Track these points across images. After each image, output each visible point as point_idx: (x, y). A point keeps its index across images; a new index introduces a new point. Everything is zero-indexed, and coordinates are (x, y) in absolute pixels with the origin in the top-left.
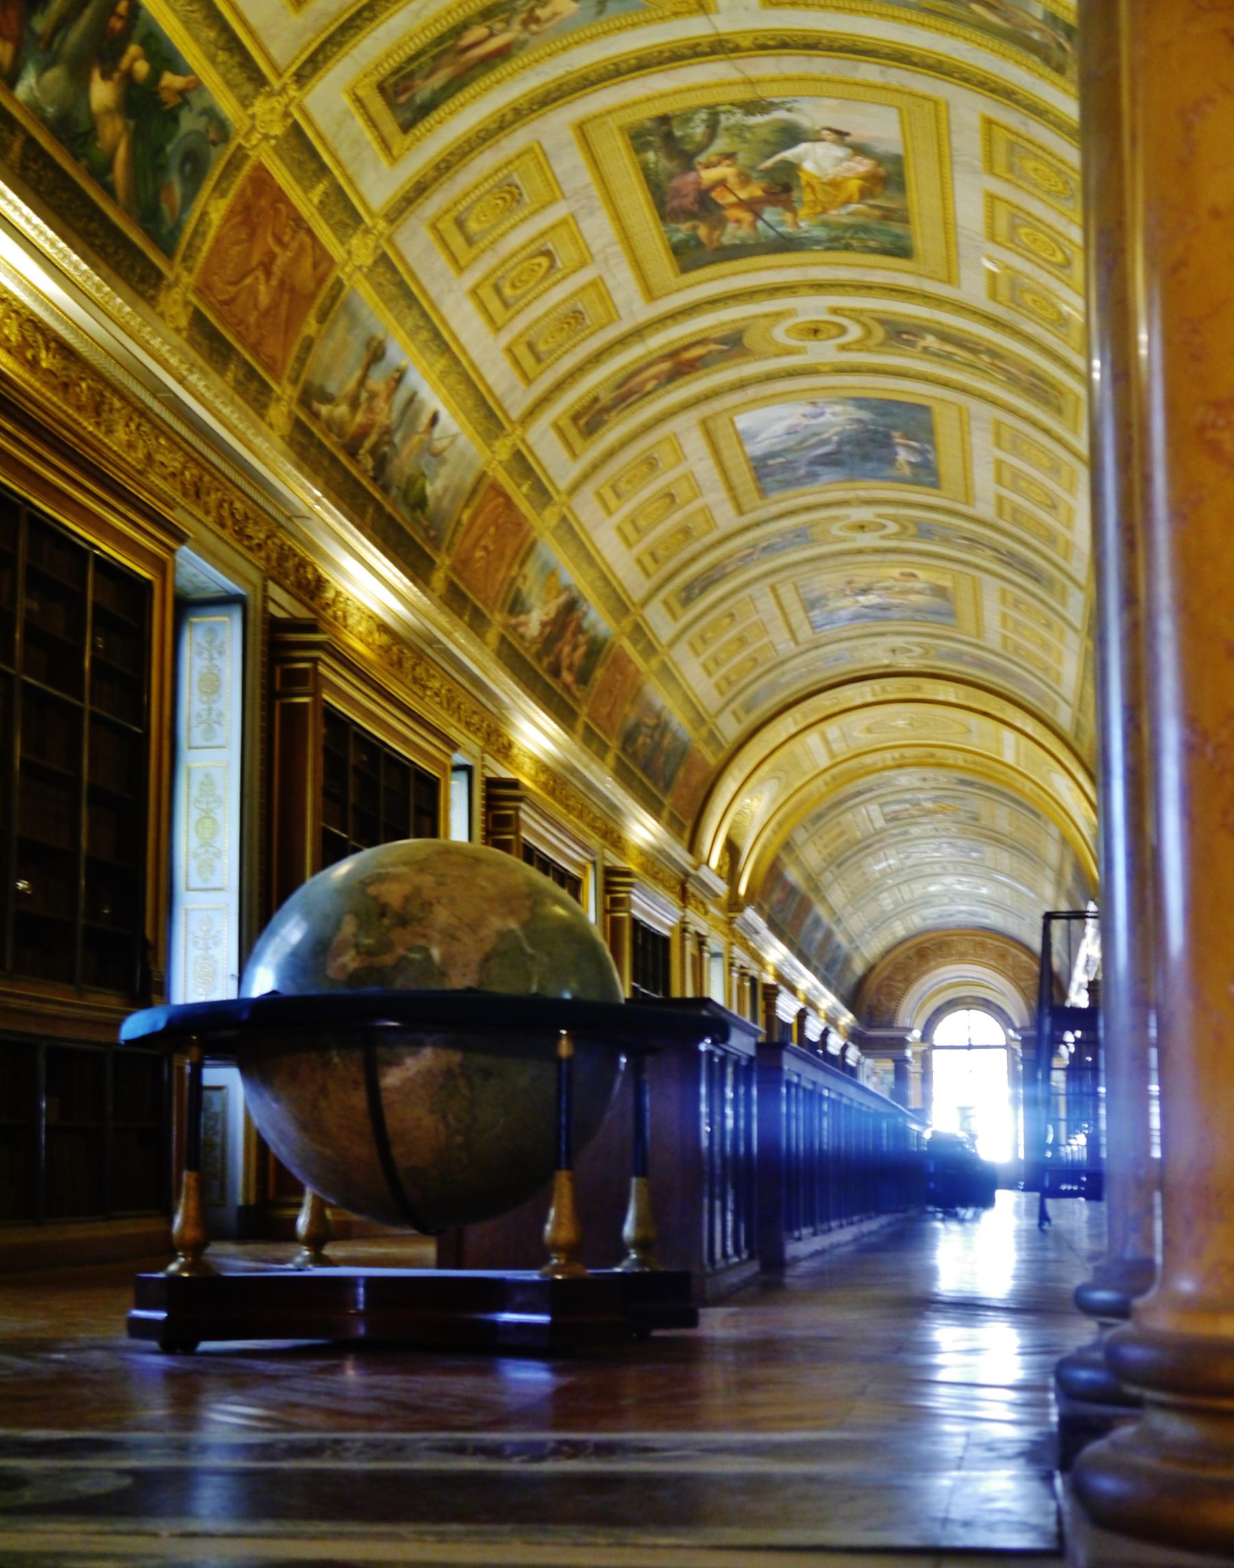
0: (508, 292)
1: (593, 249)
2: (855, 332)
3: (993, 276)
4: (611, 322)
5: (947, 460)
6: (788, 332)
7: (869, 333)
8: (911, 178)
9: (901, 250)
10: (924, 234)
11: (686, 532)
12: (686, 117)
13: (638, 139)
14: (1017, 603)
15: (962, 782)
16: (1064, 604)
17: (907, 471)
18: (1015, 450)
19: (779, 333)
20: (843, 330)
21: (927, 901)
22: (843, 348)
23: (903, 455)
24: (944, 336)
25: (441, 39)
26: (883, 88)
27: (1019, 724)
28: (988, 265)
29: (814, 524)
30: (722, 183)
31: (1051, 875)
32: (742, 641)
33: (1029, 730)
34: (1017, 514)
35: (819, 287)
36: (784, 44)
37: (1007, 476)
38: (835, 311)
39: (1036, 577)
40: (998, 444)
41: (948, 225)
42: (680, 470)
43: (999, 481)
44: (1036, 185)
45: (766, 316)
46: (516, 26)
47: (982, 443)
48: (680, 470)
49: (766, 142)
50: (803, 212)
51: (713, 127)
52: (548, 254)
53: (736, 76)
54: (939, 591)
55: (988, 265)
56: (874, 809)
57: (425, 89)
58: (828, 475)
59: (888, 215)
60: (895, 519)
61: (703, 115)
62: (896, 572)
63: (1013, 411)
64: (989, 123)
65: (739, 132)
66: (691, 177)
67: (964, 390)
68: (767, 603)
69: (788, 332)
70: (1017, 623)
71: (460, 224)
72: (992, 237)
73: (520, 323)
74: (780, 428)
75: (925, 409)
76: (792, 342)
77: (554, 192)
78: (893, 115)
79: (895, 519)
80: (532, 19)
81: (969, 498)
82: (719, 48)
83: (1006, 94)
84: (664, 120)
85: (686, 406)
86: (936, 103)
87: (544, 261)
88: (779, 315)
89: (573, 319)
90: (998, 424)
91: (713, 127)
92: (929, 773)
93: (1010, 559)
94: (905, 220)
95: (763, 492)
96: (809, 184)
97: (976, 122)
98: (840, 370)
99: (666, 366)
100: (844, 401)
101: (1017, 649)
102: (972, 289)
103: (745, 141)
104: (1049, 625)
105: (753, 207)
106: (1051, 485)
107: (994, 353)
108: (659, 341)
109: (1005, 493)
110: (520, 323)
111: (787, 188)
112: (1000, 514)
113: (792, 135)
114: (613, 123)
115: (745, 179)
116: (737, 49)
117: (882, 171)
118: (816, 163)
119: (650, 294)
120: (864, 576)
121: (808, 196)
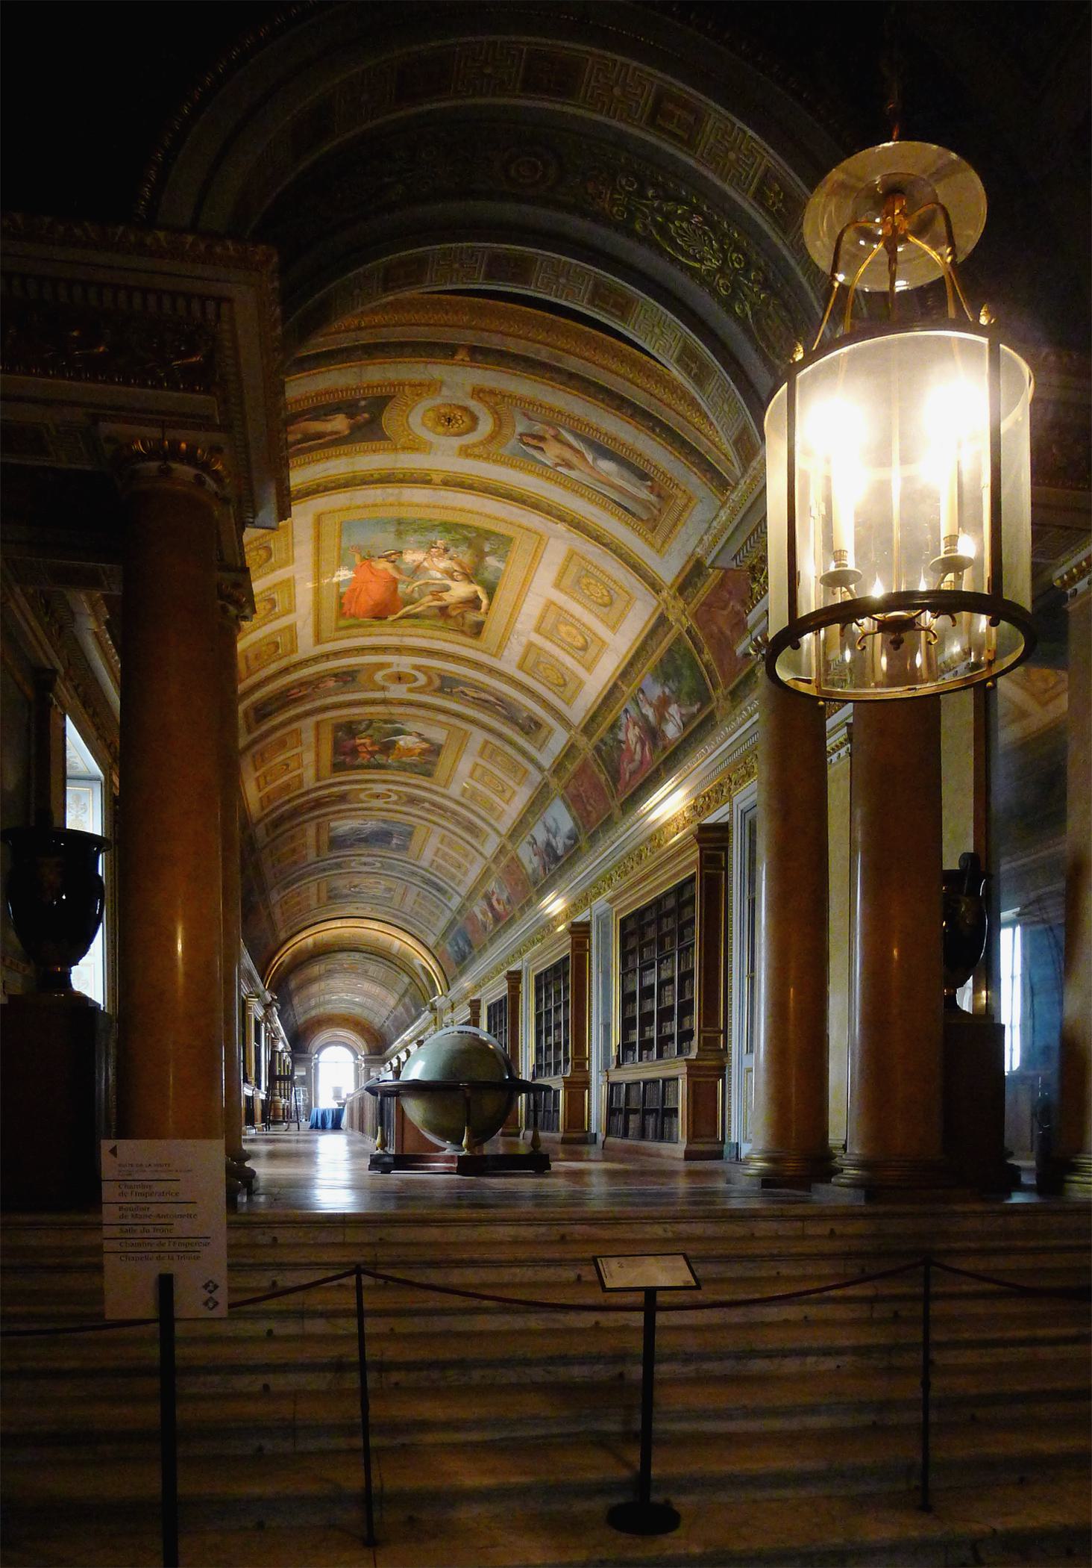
0: (268, 778)
1: (305, 763)
2: (394, 798)
3: (465, 789)
4: (299, 789)
5: (415, 844)
6: (366, 796)
7: (400, 797)
8: (443, 752)
9: (428, 774)
10: (441, 772)
11: (295, 863)
12: (360, 722)
13: (338, 727)
14: (424, 898)
15: (365, 958)
16: (450, 900)
17: (394, 846)
18: (450, 845)
19: (362, 796)
20: (390, 797)
21: (329, 1002)
22: (386, 803)
23: (395, 841)
24: (434, 804)
25: (282, 693)
26: (448, 724)
27: (405, 940)
28: (465, 784)
29: (345, 862)
30: (364, 744)
31: (397, 997)
32: (298, 903)
33: (409, 942)
34: (439, 867)
35: (385, 782)
36: (411, 704)
37: (440, 853)
38: (389, 790)
39: (439, 889)
40: (442, 842)
41: (453, 769)
42: (302, 841)
43: (436, 854)
44: (499, 765)
45: (361, 789)
46: (311, 689)
47: (434, 842)
48: (302, 841)
49: (388, 733)
50: (391, 757)
51: (369, 727)
52: (287, 765)
53: (387, 711)
54: (390, 890)
55: (465, 784)
56: (323, 967)
57: (269, 708)
58: (363, 844)
59: (430, 762)
60: (380, 862)
61: (366, 722)
62: (371, 881)
63: (454, 833)
64: (487, 742)
65: (379, 729)
66: (352, 741)
67: (435, 823)
68: (313, 890)
69: (366, 796)
70: (421, 904)
71: (262, 755)
72: (471, 776)
73: (267, 790)
74: (348, 827)
75: (414, 827)
76: (366, 799)
77: (300, 743)
78: (447, 732)
79: (380, 862)
80: (317, 687)
81: (418, 858)
82: (385, 702)
83: (500, 736)
84: (351, 722)
85: (313, 819)
86: (466, 732)
87: (285, 767)
88: (365, 789)
89: (286, 788)
90: (444, 836)
91: (369, 727)
92: (353, 953)
93: (428, 882)
94: (434, 764)
95: (330, 849)
96: (399, 749)
97: (481, 741)
98: (380, 810)
99: (313, 804)
100: (378, 820)
101: (417, 913)
102: (454, 790)
103: (379, 732)
104: (437, 907)
105: (372, 754)
106: (461, 859)
107: (454, 813)
108: (314, 795)
109: (436, 859)
110: (267, 790)
111: (389, 748)
112: (431, 866)
113: (400, 732)
114: (334, 722)
115: (373, 744)
116: (392, 703)
117: (432, 748)
118: (406, 743)
119: (318, 779)
120: (356, 881)
121: (396, 752)
